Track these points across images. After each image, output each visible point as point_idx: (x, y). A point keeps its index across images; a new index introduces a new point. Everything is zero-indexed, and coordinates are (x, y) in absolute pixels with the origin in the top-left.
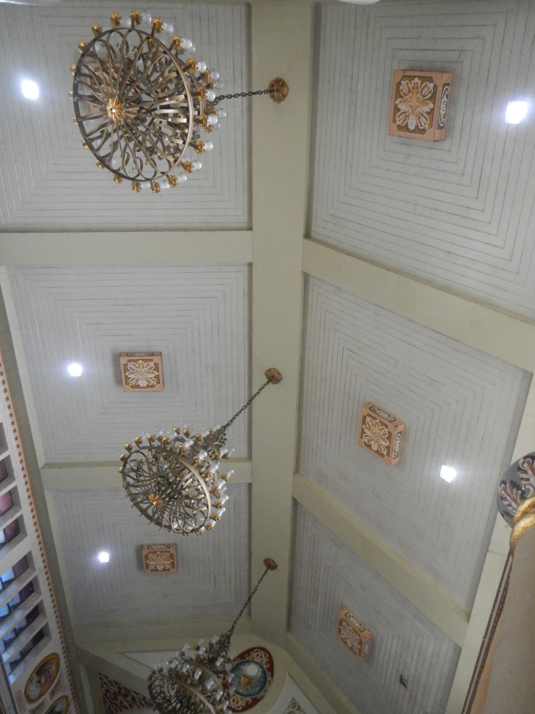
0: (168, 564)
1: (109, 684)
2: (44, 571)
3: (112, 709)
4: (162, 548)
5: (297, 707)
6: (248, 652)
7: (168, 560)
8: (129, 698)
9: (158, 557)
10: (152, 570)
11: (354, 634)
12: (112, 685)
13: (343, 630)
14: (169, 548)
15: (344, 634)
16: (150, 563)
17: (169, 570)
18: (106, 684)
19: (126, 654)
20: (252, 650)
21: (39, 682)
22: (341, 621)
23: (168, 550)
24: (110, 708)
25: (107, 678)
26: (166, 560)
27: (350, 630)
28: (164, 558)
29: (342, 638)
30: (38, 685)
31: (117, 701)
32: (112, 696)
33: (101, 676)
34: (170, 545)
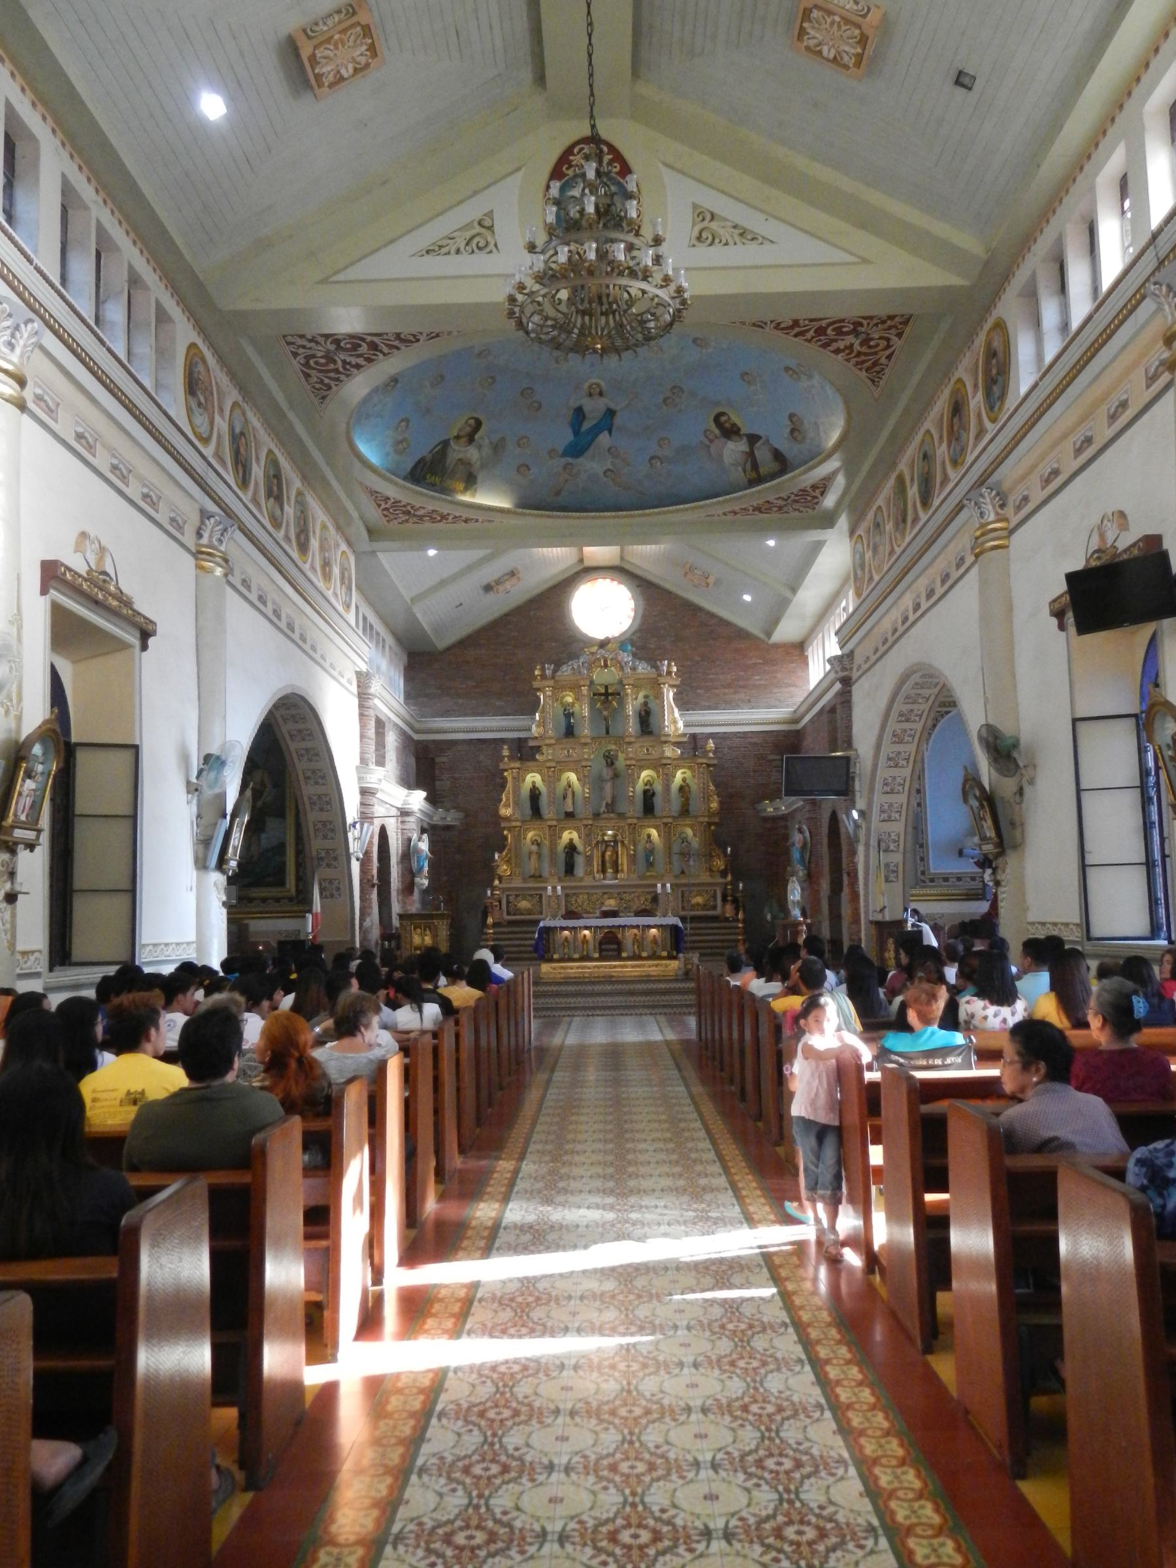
0: (362, 55)
1: (312, 345)
2: (102, 203)
3: (327, 381)
4: (340, 22)
5: (708, 217)
6: (564, 159)
7: (362, 44)
8: (364, 348)
9: (337, 48)
10: (331, 86)
11: (844, 28)
12: (317, 343)
13: (813, 28)
14: (354, 13)
15: (815, 35)
16: (324, 70)
17: (367, 65)
18: (304, 347)
19: (335, 278)
20: (569, 151)
21: (200, 404)
22: (806, 14)
23: (355, 19)
24: (322, 382)
25: (302, 336)
26: (355, 46)
27: (833, 23)
28: (351, 43)
29: (808, 48)
31: (335, 362)
32: (323, 361)
33: (289, 339)
34: (351, 6)
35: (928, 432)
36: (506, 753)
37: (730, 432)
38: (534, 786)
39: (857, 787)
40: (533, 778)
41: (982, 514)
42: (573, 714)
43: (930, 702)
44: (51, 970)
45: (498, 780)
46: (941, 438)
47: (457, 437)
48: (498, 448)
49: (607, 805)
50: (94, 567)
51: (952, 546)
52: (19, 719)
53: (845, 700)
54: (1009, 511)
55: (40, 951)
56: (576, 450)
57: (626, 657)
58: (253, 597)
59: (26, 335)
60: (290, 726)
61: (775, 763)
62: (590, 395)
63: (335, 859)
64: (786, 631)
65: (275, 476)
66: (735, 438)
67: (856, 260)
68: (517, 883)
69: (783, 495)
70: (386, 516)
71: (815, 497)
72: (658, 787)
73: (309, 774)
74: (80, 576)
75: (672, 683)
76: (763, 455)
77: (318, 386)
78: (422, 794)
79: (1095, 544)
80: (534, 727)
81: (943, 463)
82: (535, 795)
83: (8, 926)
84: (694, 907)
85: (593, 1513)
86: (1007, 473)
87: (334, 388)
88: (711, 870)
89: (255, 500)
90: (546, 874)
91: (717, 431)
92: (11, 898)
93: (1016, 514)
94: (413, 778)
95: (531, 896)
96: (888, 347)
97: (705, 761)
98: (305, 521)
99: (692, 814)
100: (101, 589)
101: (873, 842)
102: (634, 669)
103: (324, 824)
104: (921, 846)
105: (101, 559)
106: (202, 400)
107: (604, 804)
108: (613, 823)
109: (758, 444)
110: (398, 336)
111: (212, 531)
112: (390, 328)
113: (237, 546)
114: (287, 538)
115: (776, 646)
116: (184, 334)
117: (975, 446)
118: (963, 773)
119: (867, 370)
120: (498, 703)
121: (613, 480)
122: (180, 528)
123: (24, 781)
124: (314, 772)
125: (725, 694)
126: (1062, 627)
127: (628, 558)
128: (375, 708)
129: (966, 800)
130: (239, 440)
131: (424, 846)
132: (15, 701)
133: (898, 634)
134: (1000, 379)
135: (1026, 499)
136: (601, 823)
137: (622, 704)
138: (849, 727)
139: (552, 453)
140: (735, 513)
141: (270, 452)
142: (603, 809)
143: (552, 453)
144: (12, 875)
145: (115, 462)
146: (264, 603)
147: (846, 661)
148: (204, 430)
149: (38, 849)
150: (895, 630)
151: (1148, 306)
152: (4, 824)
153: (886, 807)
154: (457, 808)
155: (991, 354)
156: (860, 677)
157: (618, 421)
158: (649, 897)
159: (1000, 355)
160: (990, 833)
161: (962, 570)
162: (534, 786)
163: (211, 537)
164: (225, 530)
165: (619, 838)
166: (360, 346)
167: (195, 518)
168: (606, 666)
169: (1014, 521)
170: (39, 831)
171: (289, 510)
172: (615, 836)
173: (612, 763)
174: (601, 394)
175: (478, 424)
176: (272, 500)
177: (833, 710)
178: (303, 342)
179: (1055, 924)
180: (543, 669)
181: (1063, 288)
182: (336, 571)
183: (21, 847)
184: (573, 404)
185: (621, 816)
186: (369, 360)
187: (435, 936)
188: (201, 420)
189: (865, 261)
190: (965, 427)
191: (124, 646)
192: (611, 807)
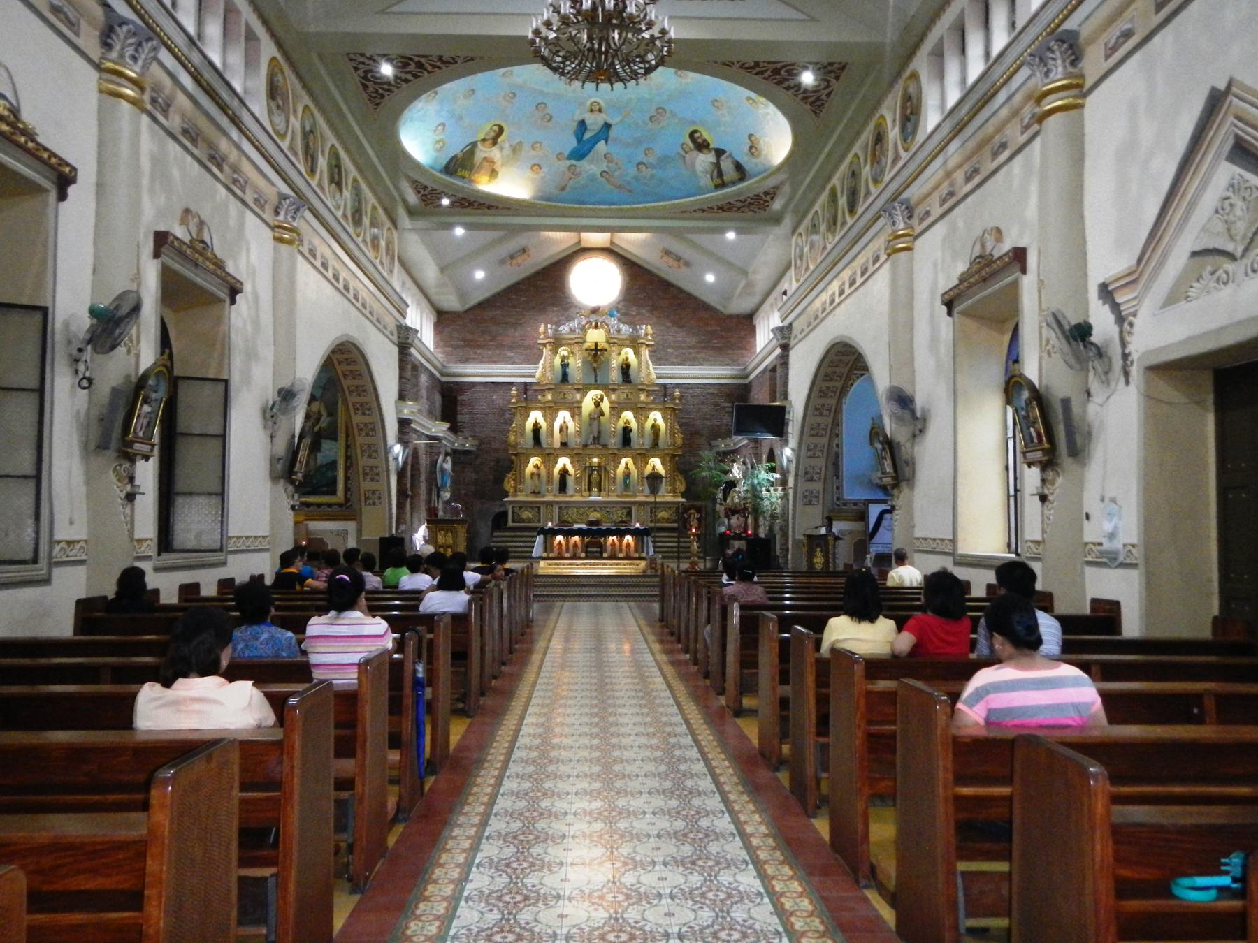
1: (371, 62)
3: (381, 91)
8: (412, 67)
18: (363, 63)
21: (278, 107)
24: (377, 91)
25: (362, 55)
30: (279, 112)
33: (352, 56)
35: (856, 155)
36: (514, 391)
37: (702, 146)
39: (790, 430)
40: (536, 416)
41: (894, 223)
43: (849, 365)
44: (159, 554)
45: (508, 416)
46: (866, 161)
47: (484, 140)
48: (516, 150)
49: (594, 438)
50: (195, 236)
51: (871, 245)
52: (138, 356)
53: (784, 360)
54: (915, 221)
55: (151, 540)
56: (579, 154)
57: (613, 322)
58: (318, 264)
59: (146, 50)
60: (345, 367)
61: (727, 409)
62: (592, 111)
63: (378, 474)
64: (739, 306)
65: (336, 166)
66: (705, 151)
67: (806, 17)
68: (521, 498)
69: (742, 198)
70: (424, 201)
71: (766, 201)
72: (634, 425)
73: (358, 406)
74: (185, 244)
76: (726, 165)
77: (374, 95)
78: (446, 426)
79: (977, 251)
80: (538, 375)
81: (867, 180)
82: (536, 429)
83: (128, 519)
84: (659, 521)
85: (588, 923)
86: (914, 193)
87: (387, 98)
88: (675, 492)
89: (320, 185)
90: (543, 490)
91: (691, 145)
92: (130, 497)
93: (920, 224)
94: (438, 411)
96: (828, 86)
98: (359, 202)
100: (201, 255)
101: (801, 473)
102: (619, 331)
103: (369, 446)
104: (838, 478)
105: (200, 230)
106: (280, 103)
107: (591, 436)
108: (598, 452)
109: (723, 157)
110: (440, 58)
111: (287, 210)
112: (436, 53)
113: (306, 223)
114: (345, 216)
115: (730, 316)
116: (268, 50)
117: (890, 171)
118: (871, 422)
119: (812, 104)
121: (607, 179)
122: (262, 207)
123: (142, 405)
124: (362, 405)
125: (690, 353)
126: (950, 313)
127: (617, 241)
128: (411, 355)
129: (872, 444)
130: (308, 135)
131: (448, 466)
132: (135, 342)
133: (826, 313)
134: (913, 118)
135: (928, 213)
136: (588, 452)
137: (608, 361)
138: (786, 384)
139: (559, 156)
140: (703, 211)
141: (333, 146)
142: (591, 440)
143: (559, 156)
144: (131, 479)
145: (213, 153)
146: (326, 269)
147: (785, 332)
148: (281, 127)
149: (151, 460)
150: (824, 309)
151: (1024, 72)
152: (127, 438)
153: (812, 446)
154: (474, 437)
155: (907, 98)
156: (797, 344)
157: (613, 133)
158: (625, 511)
159: (914, 100)
160: (889, 469)
161: (877, 265)
163: (286, 214)
164: (298, 209)
165: (603, 464)
166: (409, 64)
167: (274, 200)
168: (596, 327)
169: (918, 230)
170: (153, 446)
171: (347, 193)
172: (599, 463)
174: (600, 111)
175: (501, 130)
176: (333, 185)
177: (774, 370)
178: (362, 59)
179: (934, 540)
180: (546, 328)
181: (963, 51)
182: (383, 243)
183: (138, 457)
184: (578, 117)
185: (605, 446)
186: (416, 76)
187: (455, 537)
188: (279, 119)
189: (813, 19)
190: (884, 153)
191: (215, 300)
192: (597, 440)
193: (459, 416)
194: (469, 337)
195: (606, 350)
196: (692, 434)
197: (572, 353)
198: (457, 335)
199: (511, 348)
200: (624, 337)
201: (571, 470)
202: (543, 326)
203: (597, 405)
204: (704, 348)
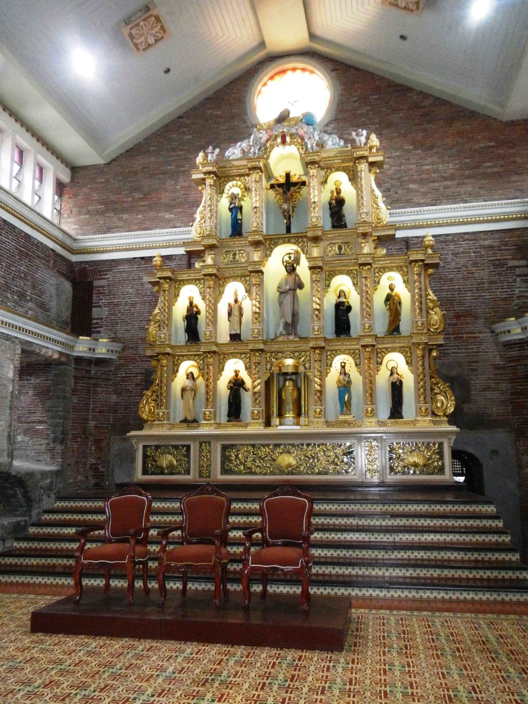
38: (191, 303)
42: (241, 208)
49: (286, 324)
61: (518, 271)
75: (371, 159)
88: (434, 414)
95: (176, 447)
97: (420, 257)
99: (403, 335)
102: (321, 145)
115: (513, 124)
120: (168, 216)
142: (281, 329)
154: (114, 340)
162: (191, 303)
165: (301, 369)
168: (284, 142)
172: (296, 367)
173: (294, 269)
193: (93, 309)
194: (113, 198)
195: (304, 183)
196: (458, 317)
197: (247, 189)
198: (95, 196)
199: (169, 208)
200: (332, 154)
201: (248, 382)
202: (201, 154)
203: (291, 268)
204: (467, 177)
